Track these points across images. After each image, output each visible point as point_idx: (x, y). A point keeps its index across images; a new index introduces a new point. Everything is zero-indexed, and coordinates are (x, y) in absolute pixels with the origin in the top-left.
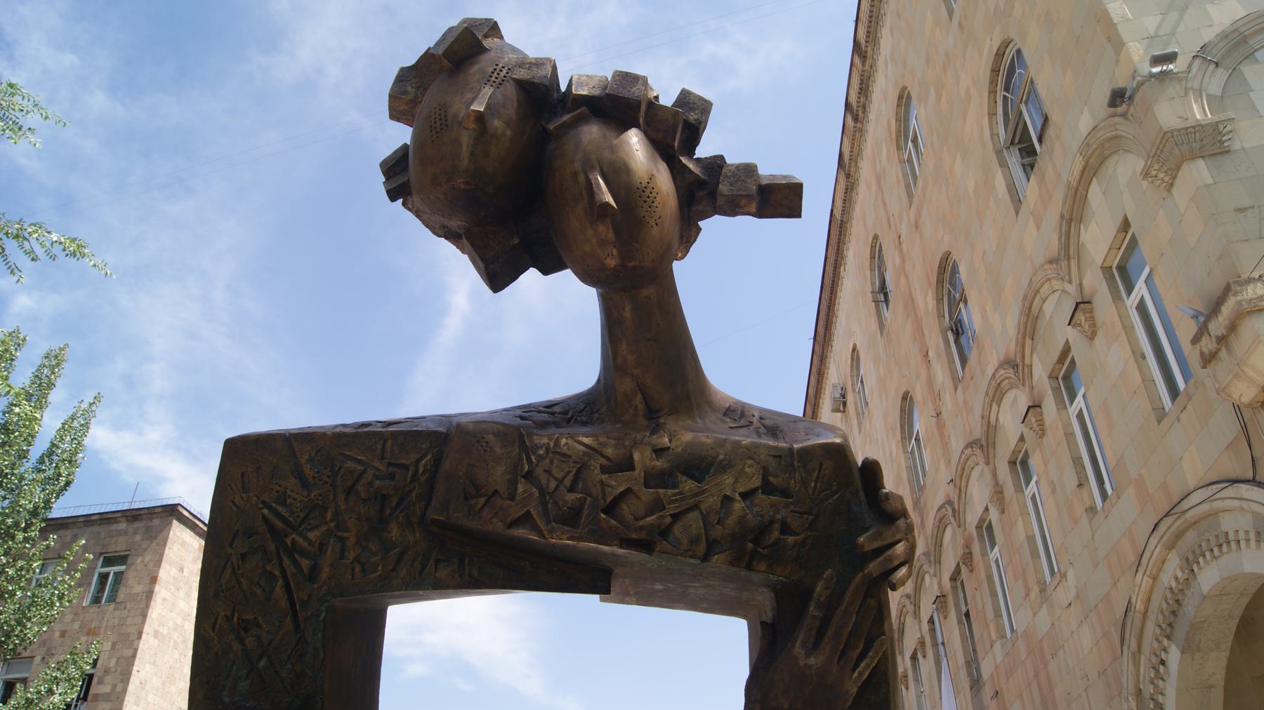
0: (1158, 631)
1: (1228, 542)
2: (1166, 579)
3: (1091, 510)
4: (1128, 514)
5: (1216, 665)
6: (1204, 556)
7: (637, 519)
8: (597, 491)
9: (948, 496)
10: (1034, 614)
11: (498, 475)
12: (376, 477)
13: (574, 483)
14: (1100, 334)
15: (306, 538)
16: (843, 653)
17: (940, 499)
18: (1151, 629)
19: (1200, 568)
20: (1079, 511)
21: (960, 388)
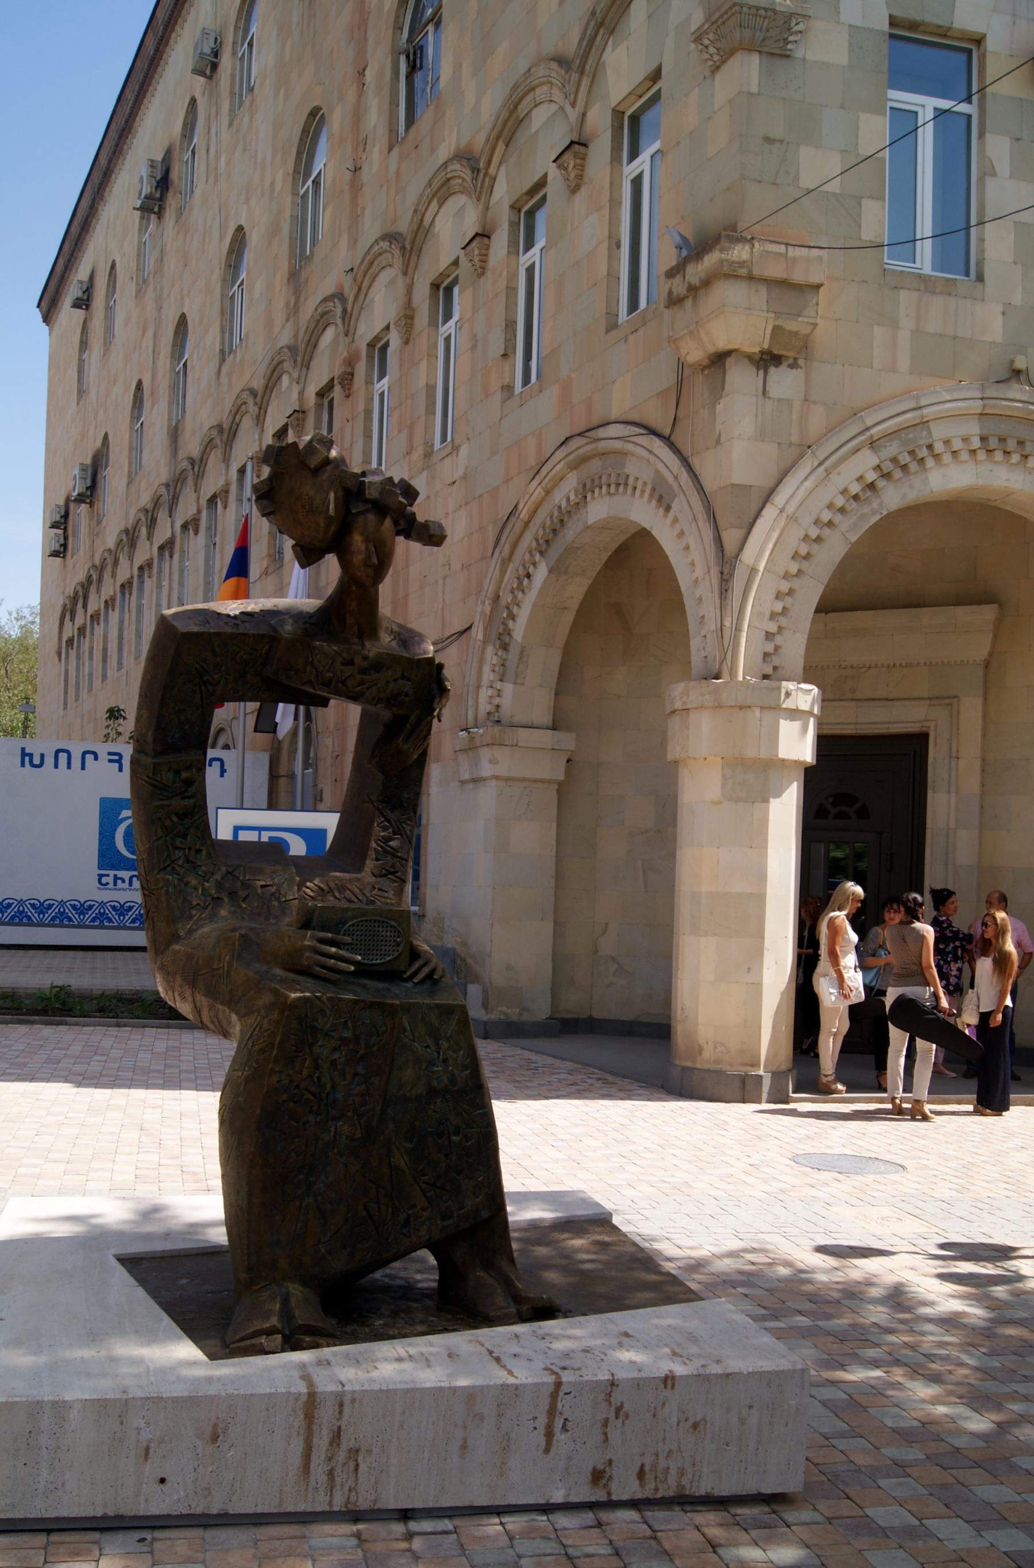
0: (534, 544)
1: (626, 484)
2: (559, 497)
4: (542, 414)
5: (576, 590)
9: (341, 287)
14: (583, 191)
17: (328, 287)
18: (528, 540)
19: (593, 498)
21: (395, 151)
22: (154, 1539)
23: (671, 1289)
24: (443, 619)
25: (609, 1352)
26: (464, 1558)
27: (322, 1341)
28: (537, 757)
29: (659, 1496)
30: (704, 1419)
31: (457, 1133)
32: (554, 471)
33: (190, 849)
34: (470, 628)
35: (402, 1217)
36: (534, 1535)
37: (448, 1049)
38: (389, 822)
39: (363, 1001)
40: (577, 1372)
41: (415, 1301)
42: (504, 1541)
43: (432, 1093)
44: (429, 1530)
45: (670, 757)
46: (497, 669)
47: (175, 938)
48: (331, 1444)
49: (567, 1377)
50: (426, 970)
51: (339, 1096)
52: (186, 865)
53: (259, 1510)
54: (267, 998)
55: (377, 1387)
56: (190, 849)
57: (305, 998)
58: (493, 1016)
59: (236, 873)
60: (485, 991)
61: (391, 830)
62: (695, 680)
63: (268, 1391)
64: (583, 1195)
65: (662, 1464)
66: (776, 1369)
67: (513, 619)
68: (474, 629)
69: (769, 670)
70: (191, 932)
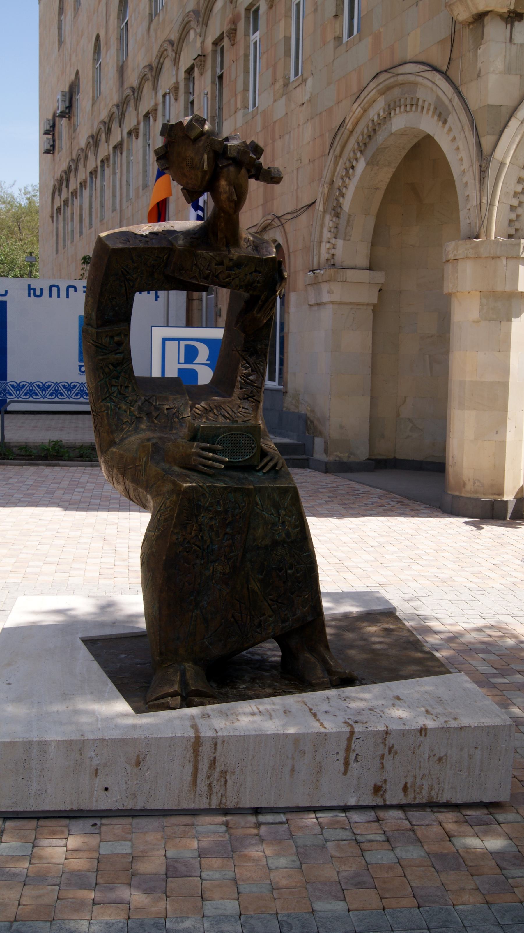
0: (356, 146)
1: (417, 105)
2: (372, 114)
3: (338, 39)
4: (361, 56)
5: (385, 176)
6: (400, 107)
7: (224, 279)
10: (275, 101)
13: (208, 267)
18: (352, 144)
19: (395, 114)
20: (330, 37)
22: (102, 825)
23: (430, 663)
24: (297, 197)
25: (387, 710)
26: (291, 841)
27: (205, 700)
28: (359, 289)
29: (416, 802)
30: (446, 755)
31: (290, 569)
32: (369, 97)
33: (121, 386)
34: (314, 202)
35: (256, 622)
36: (336, 826)
37: (285, 515)
38: (249, 364)
39: (230, 487)
40: (364, 725)
41: (266, 671)
42: (317, 829)
43: (275, 543)
44: (271, 821)
45: (446, 291)
46: (332, 230)
47: (113, 443)
48: (210, 768)
49: (358, 728)
50: (271, 464)
51: (215, 547)
52: (119, 396)
53: (166, 808)
54: (168, 487)
55: (238, 733)
56: (121, 386)
57: (192, 487)
58: (331, 459)
59: (151, 401)
60: (326, 442)
61: (250, 369)
62: (463, 239)
63: (170, 735)
64: (378, 595)
65: (418, 782)
66: (493, 724)
67: (343, 197)
68: (317, 204)
69: (513, 232)
70: (123, 439)
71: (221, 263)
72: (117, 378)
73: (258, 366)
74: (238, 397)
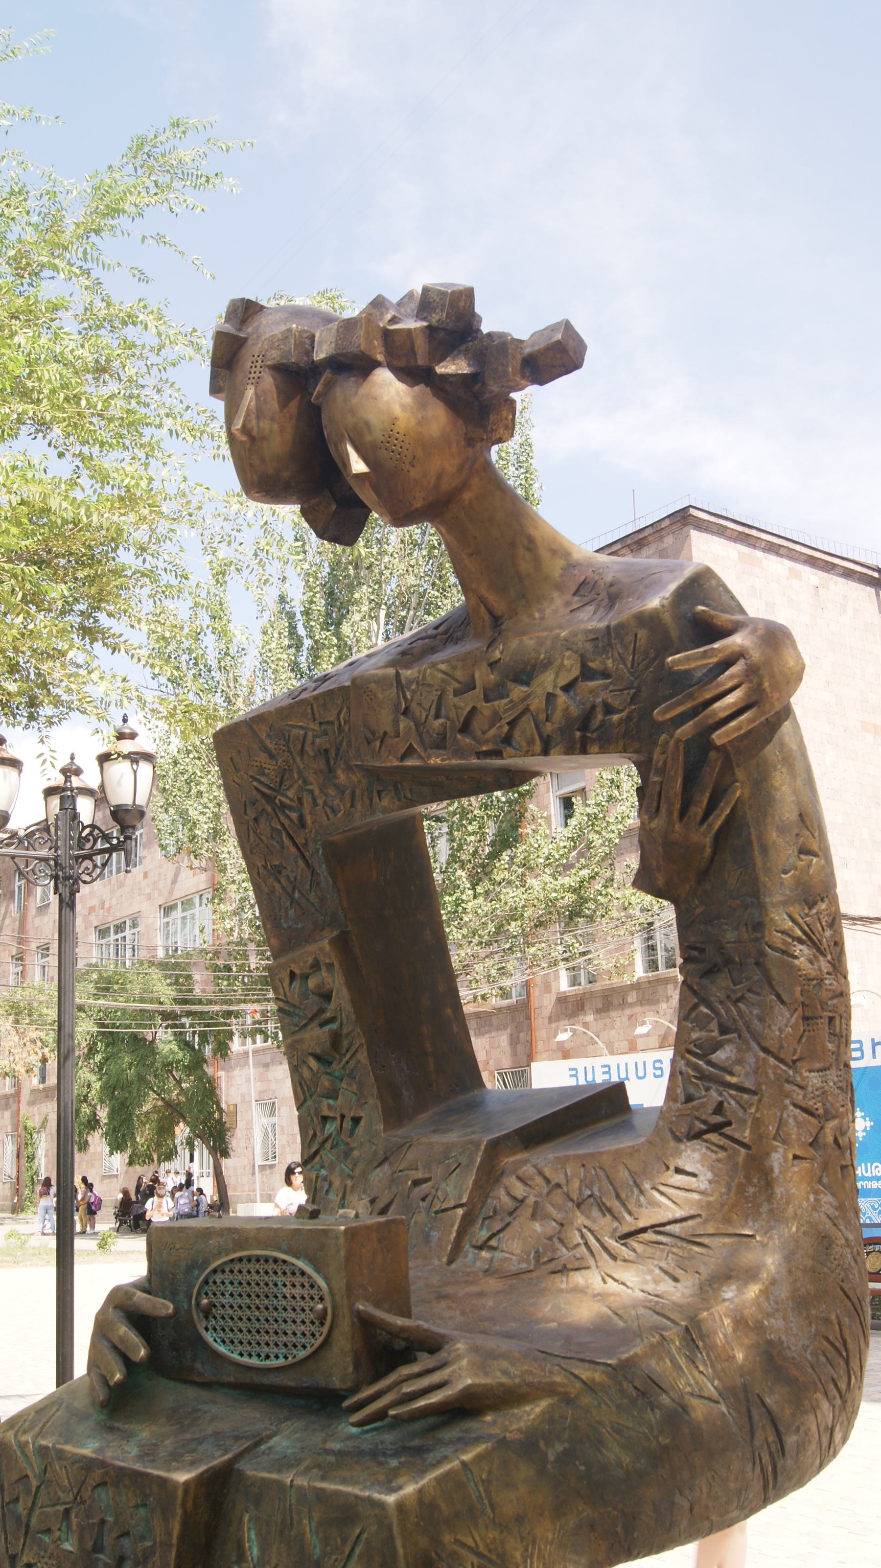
7: (484, 733)
8: (453, 714)
11: (384, 719)
12: (315, 736)
15: (287, 797)
16: (683, 813)
33: (343, 1117)
38: (709, 1006)
56: (343, 1117)
61: (714, 1025)
71: (470, 686)
72: (333, 1094)
73: (739, 1011)
74: (673, 1133)
